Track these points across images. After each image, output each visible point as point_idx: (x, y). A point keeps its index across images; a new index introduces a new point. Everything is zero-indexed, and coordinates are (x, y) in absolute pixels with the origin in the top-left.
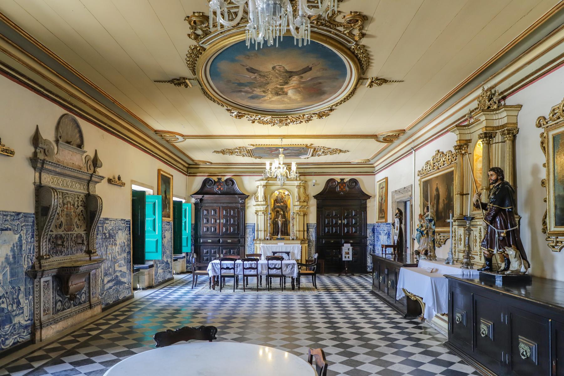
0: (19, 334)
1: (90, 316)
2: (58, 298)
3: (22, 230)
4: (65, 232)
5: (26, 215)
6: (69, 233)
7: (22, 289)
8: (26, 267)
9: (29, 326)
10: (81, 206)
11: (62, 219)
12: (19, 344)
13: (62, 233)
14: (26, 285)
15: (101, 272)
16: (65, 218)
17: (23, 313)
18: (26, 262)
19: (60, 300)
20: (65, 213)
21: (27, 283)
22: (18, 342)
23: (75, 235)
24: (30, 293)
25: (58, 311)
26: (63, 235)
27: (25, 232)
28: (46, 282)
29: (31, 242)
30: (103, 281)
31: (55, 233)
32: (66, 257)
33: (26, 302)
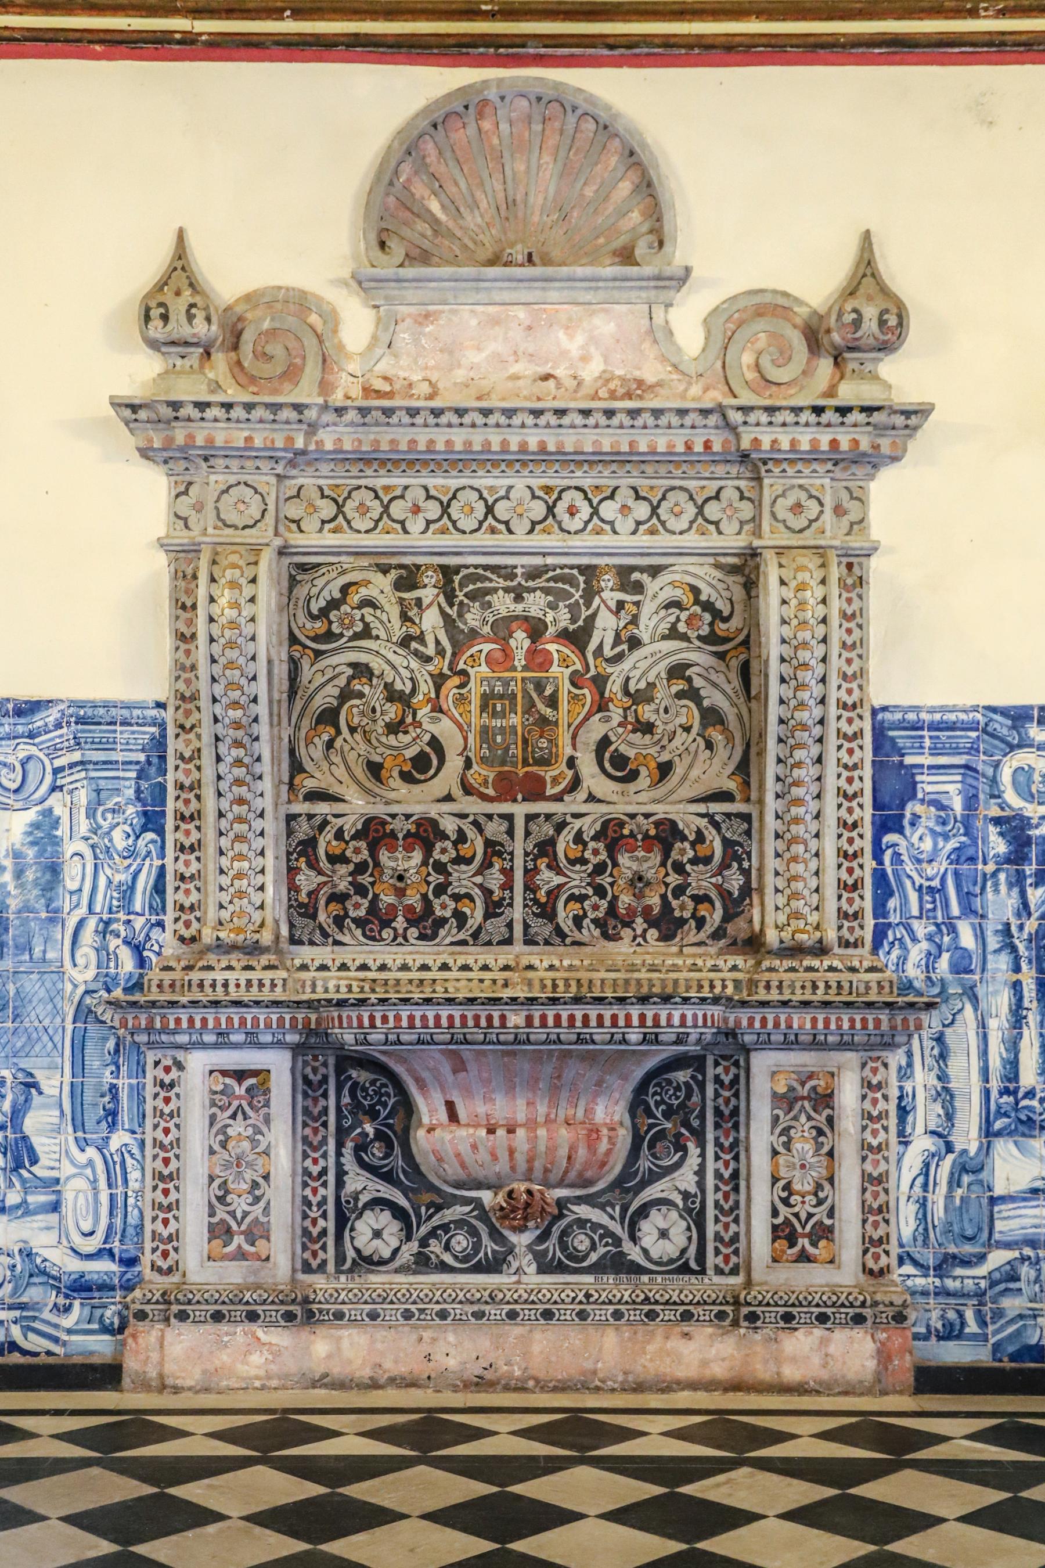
0: (22, 1307)
1: (719, 1371)
2: (357, 1181)
3: (54, 789)
4: (474, 806)
5: (86, 717)
6: (520, 810)
7: (54, 1083)
8: (83, 972)
9: (105, 1287)
10: (673, 634)
11: (444, 729)
12: (16, 1358)
13: (433, 811)
14: (79, 1065)
15: (945, 1095)
16: (476, 719)
17: (55, 1207)
18: (86, 952)
19: (378, 1203)
20: (475, 690)
21: (93, 1062)
22: (13, 1346)
23: (589, 826)
24: (112, 1116)
25: (368, 1262)
26: (449, 826)
27: (83, 797)
28: (240, 1075)
29: (131, 853)
30: (969, 1168)
31: (357, 806)
32: (475, 956)
33: (82, 1158)
